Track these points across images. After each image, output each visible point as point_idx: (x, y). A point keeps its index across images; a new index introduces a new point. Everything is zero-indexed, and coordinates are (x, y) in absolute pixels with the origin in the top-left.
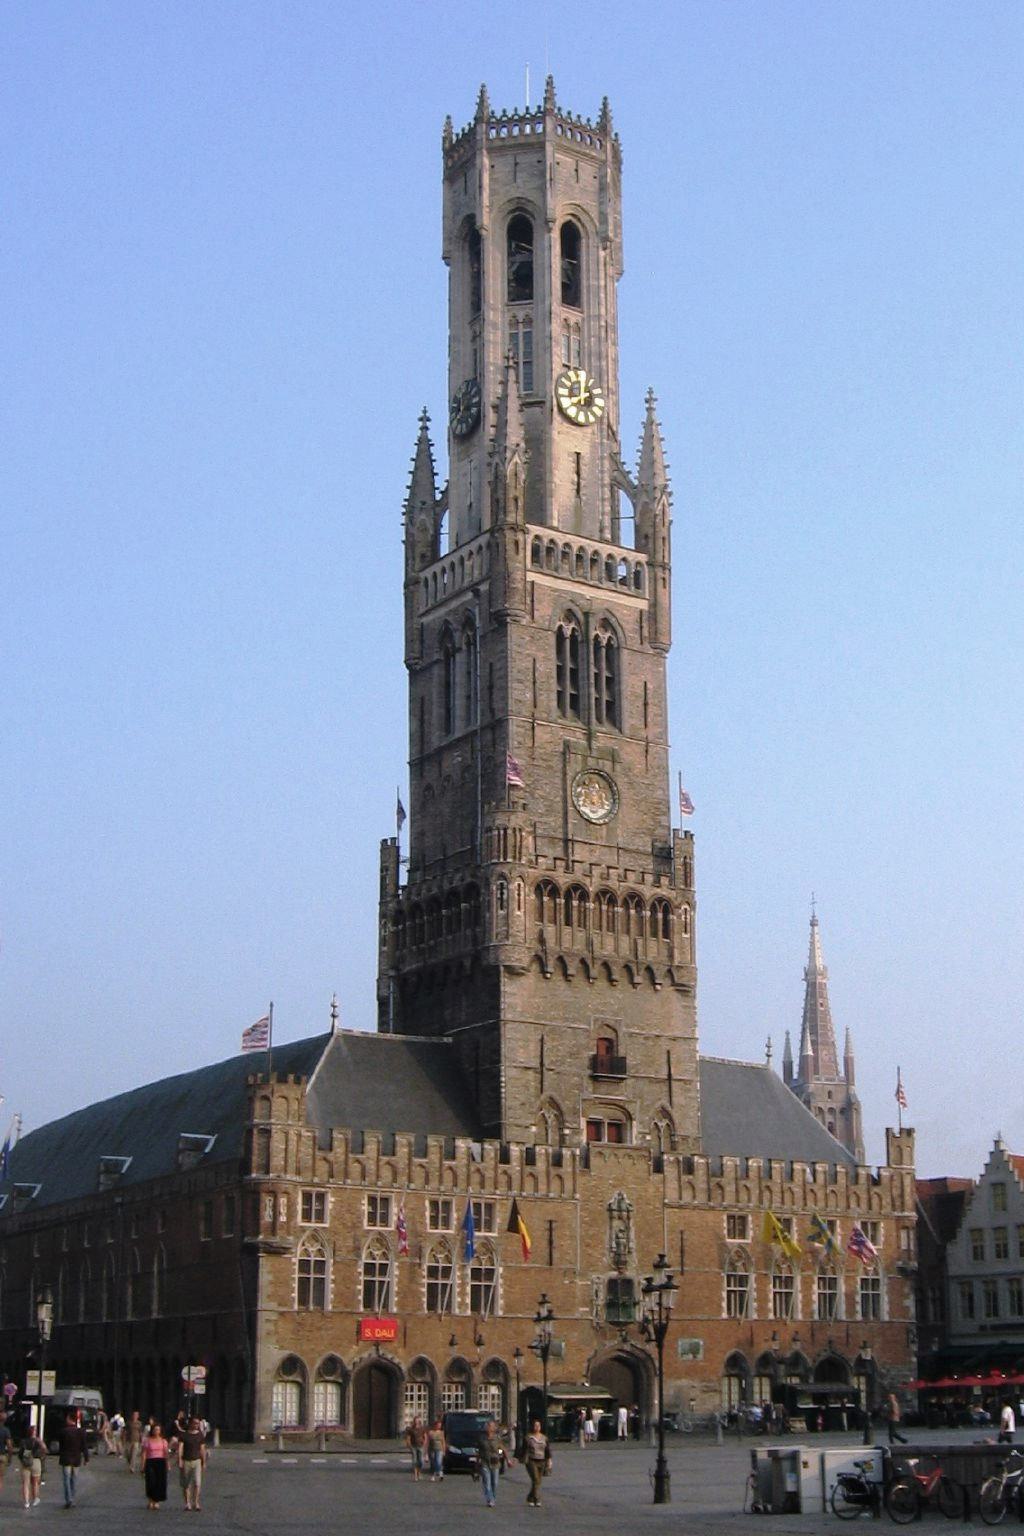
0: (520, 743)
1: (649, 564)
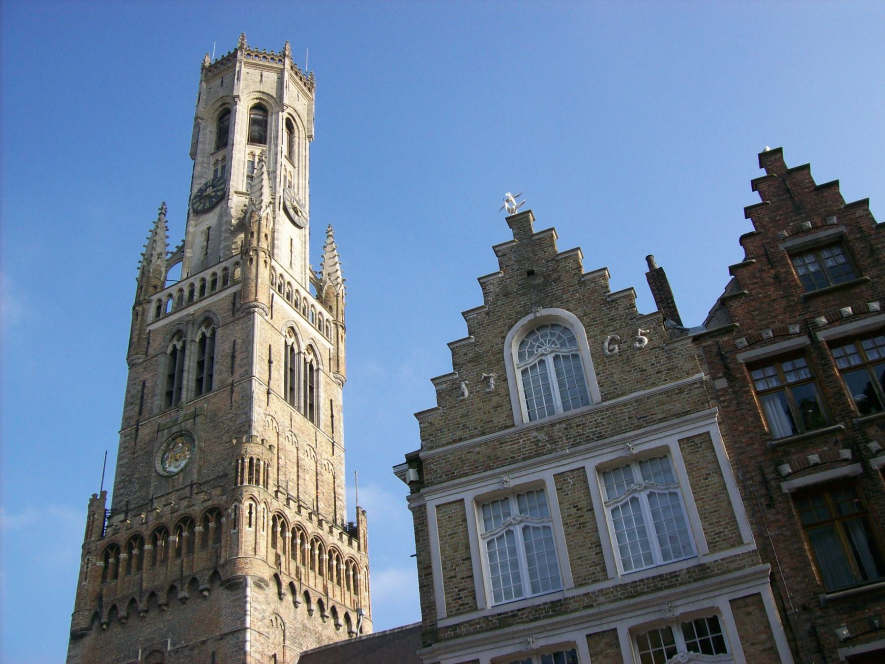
1: (242, 258)
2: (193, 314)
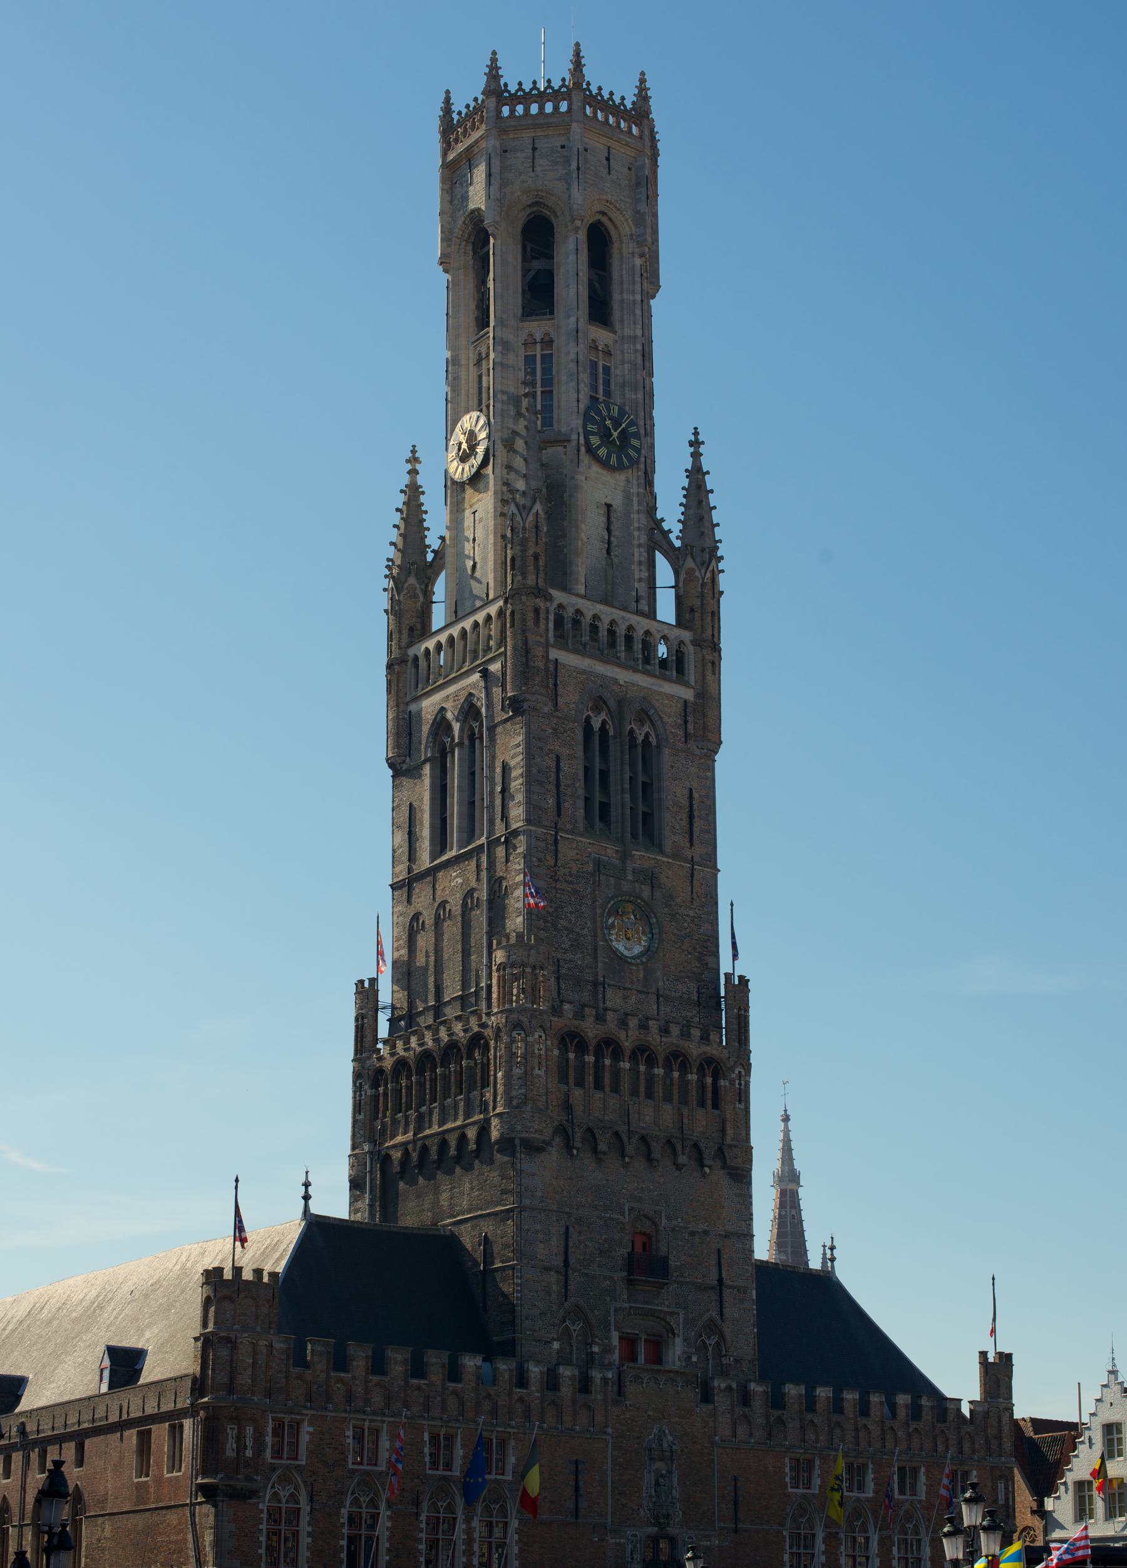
0: (540, 860)
2: (621, 685)
